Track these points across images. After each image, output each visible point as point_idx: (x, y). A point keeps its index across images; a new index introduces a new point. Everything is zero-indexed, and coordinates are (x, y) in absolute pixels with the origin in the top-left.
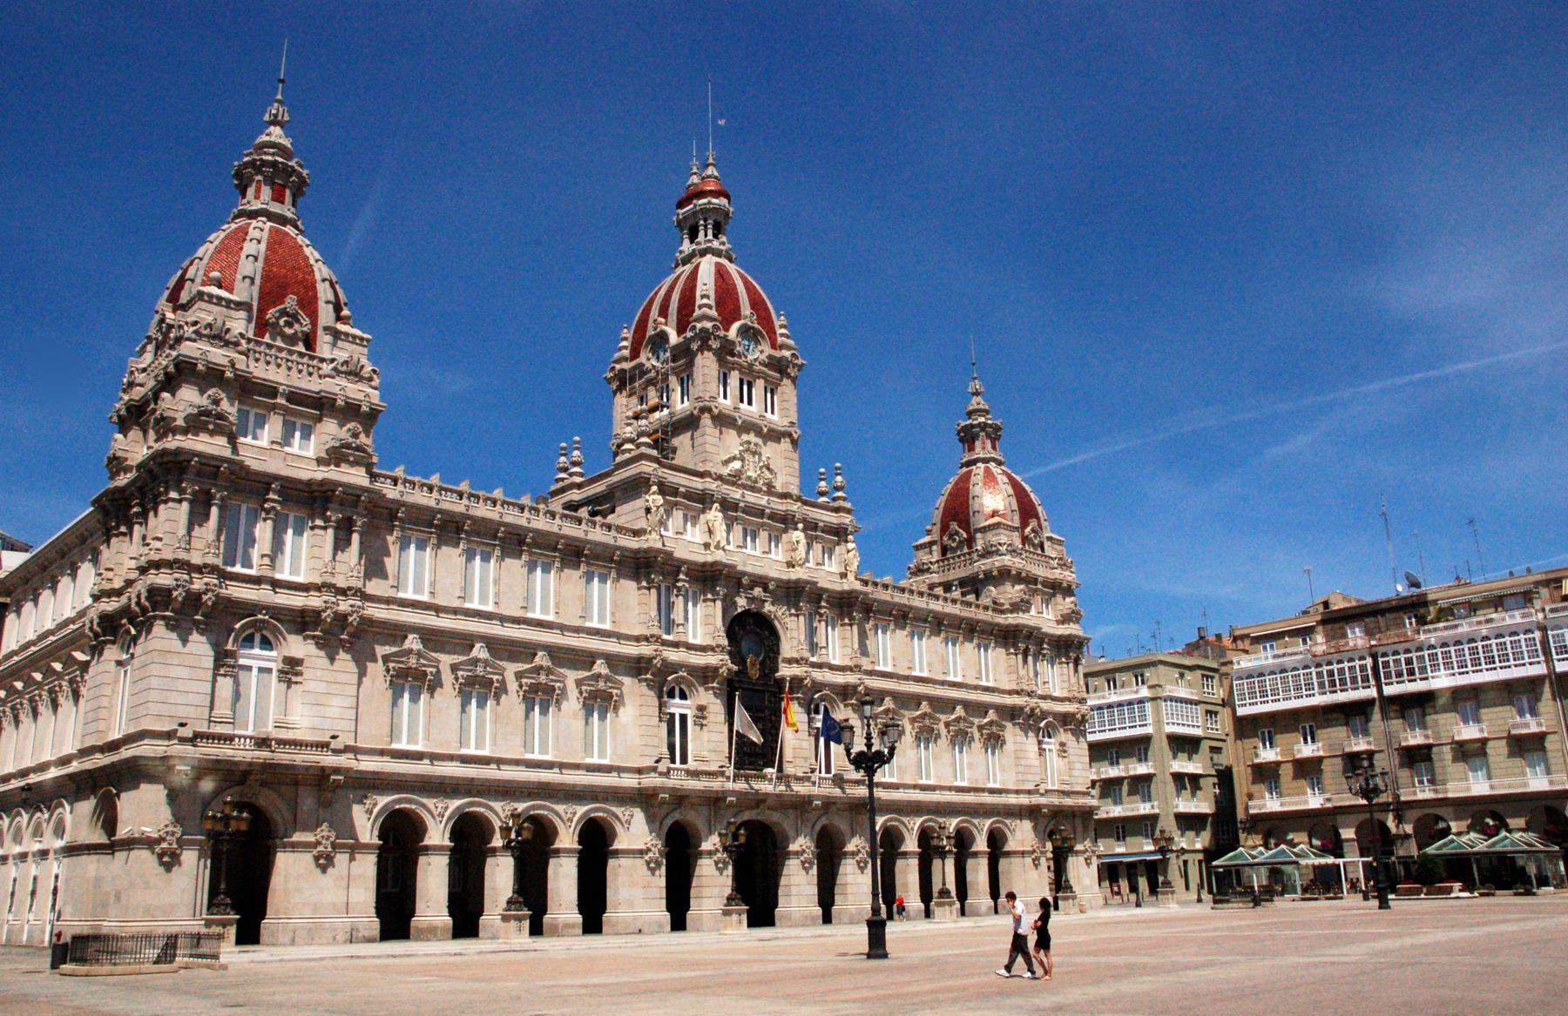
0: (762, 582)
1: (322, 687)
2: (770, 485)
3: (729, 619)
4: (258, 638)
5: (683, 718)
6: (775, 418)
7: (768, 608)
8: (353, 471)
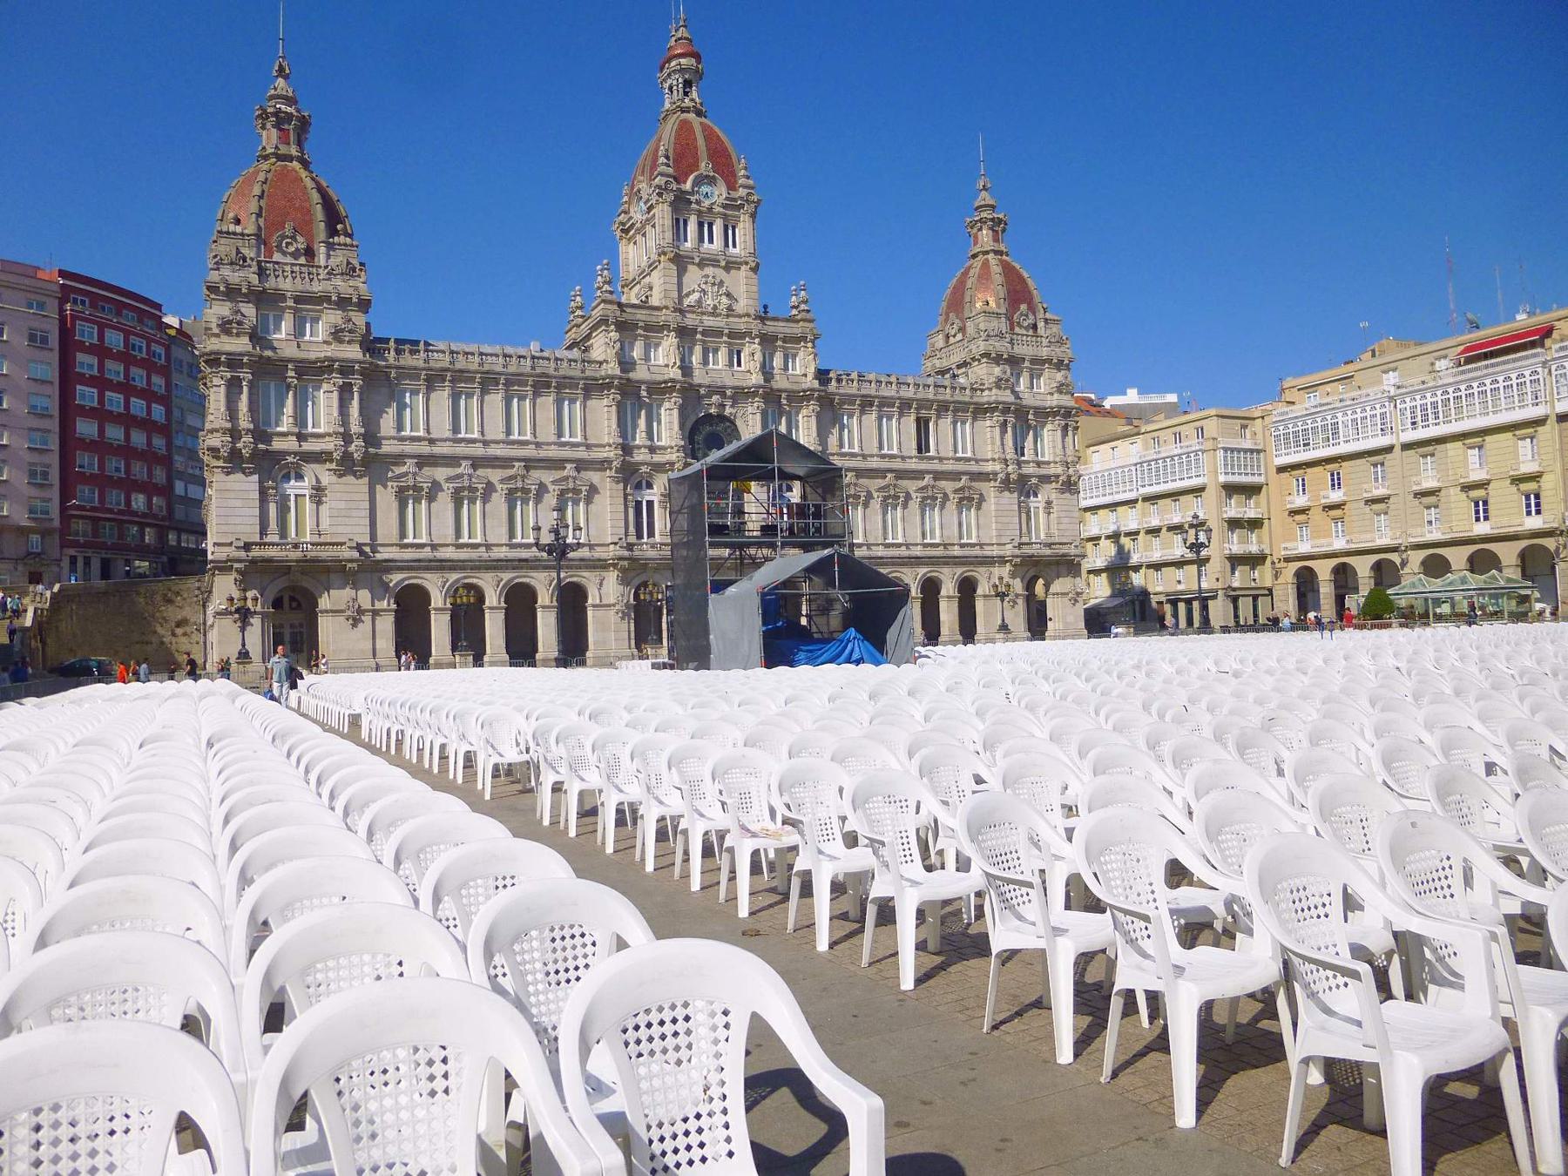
0: (720, 391)
1: (342, 505)
2: (730, 309)
3: (689, 425)
4: (293, 475)
5: (650, 504)
6: (737, 250)
7: (728, 411)
8: (349, 348)
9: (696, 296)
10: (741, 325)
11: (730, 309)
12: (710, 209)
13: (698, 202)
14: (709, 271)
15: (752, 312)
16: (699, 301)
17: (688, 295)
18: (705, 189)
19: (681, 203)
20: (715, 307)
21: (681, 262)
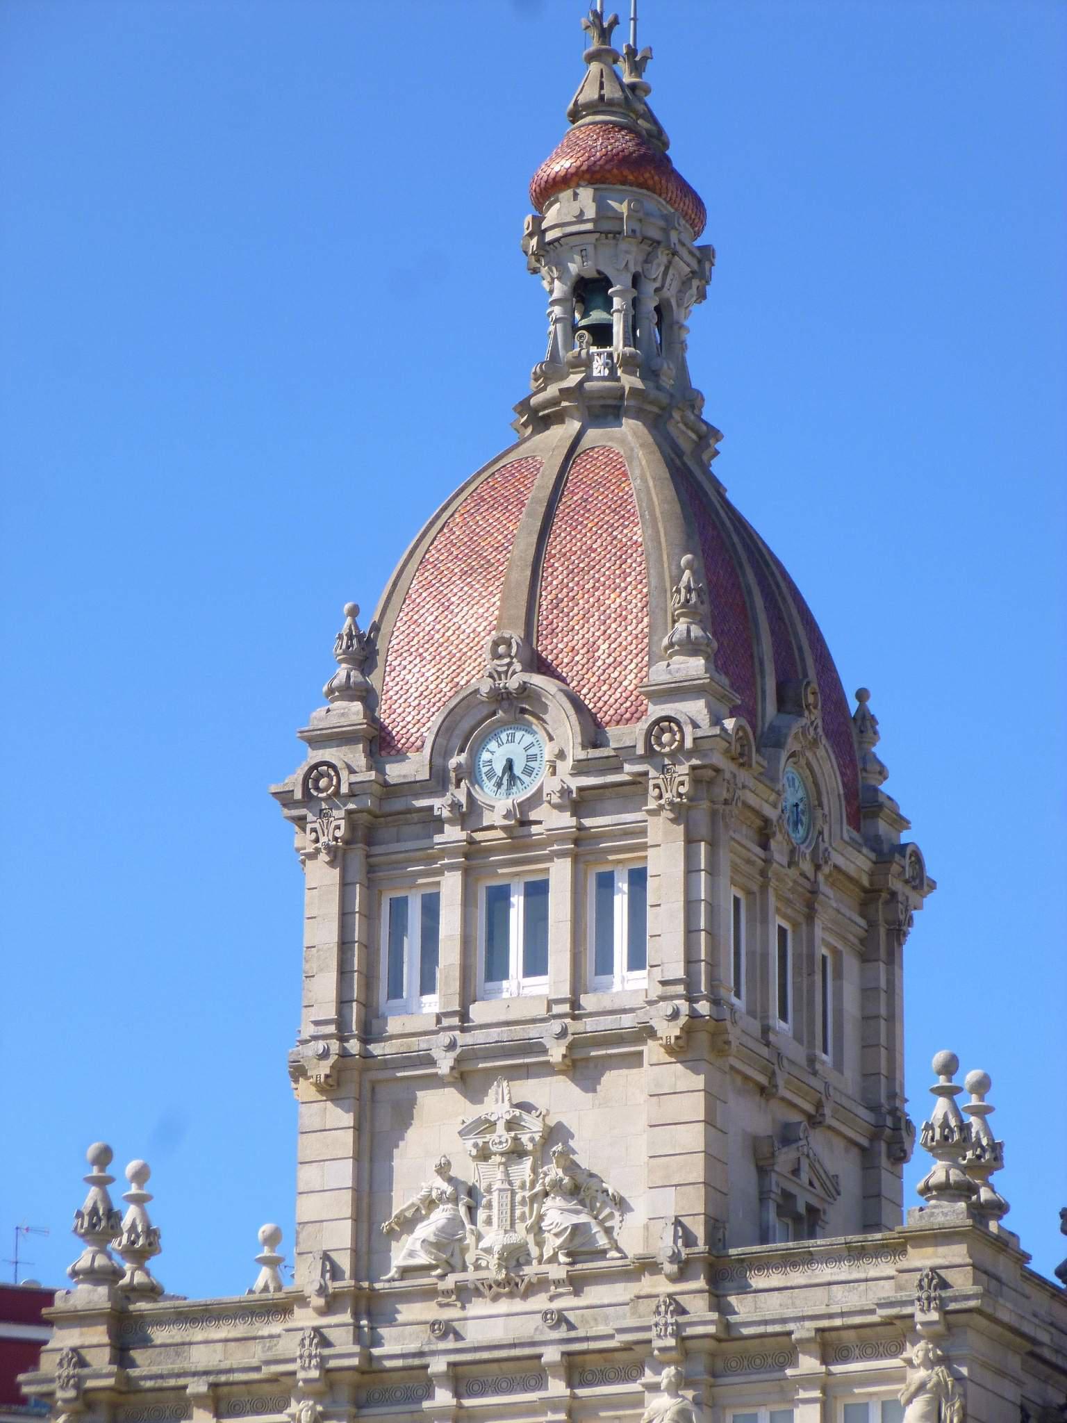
9: (440, 1216)
10: (608, 1311)
11: (579, 1247)
12: (521, 821)
13: (468, 814)
14: (496, 1105)
15: (665, 1244)
16: (449, 1248)
17: (408, 1224)
18: (495, 754)
19: (379, 837)
20: (515, 1257)
21: (373, 1093)
